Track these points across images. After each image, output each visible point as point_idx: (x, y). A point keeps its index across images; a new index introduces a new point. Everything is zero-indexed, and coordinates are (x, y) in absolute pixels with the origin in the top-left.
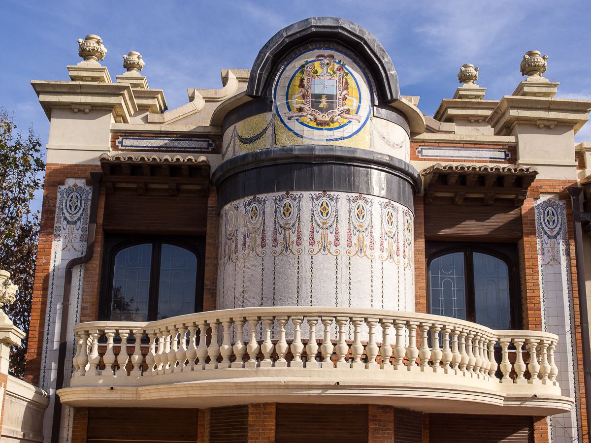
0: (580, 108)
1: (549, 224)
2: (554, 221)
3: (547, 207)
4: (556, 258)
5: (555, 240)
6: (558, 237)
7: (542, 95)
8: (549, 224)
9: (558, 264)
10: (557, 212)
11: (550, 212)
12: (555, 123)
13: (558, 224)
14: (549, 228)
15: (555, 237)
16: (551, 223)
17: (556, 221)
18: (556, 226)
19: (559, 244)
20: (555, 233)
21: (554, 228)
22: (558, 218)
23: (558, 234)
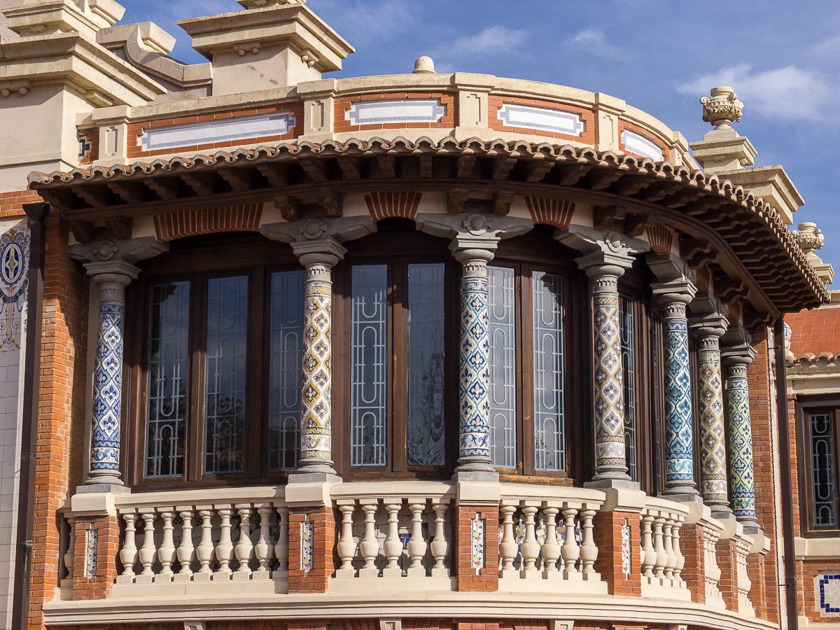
0: (55, 51)
1: (8, 275)
2: (17, 269)
3: (8, 244)
4: (13, 337)
5: (15, 304)
6: (21, 298)
7: (39, 29)
8: (8, 275)
9: (15, 348)
10: (22, 252)
11: (12, 254)
12: (25, 84)
13: (22, 273)
14: (7, 283)
15: (16, 298)
16: (11, 274)
17: (20, 269)
18: (20, 278)
19: (20, 311)
20: (16, 291)
21: (16, 282)
22: (24, 262)
23: (21, 292)
